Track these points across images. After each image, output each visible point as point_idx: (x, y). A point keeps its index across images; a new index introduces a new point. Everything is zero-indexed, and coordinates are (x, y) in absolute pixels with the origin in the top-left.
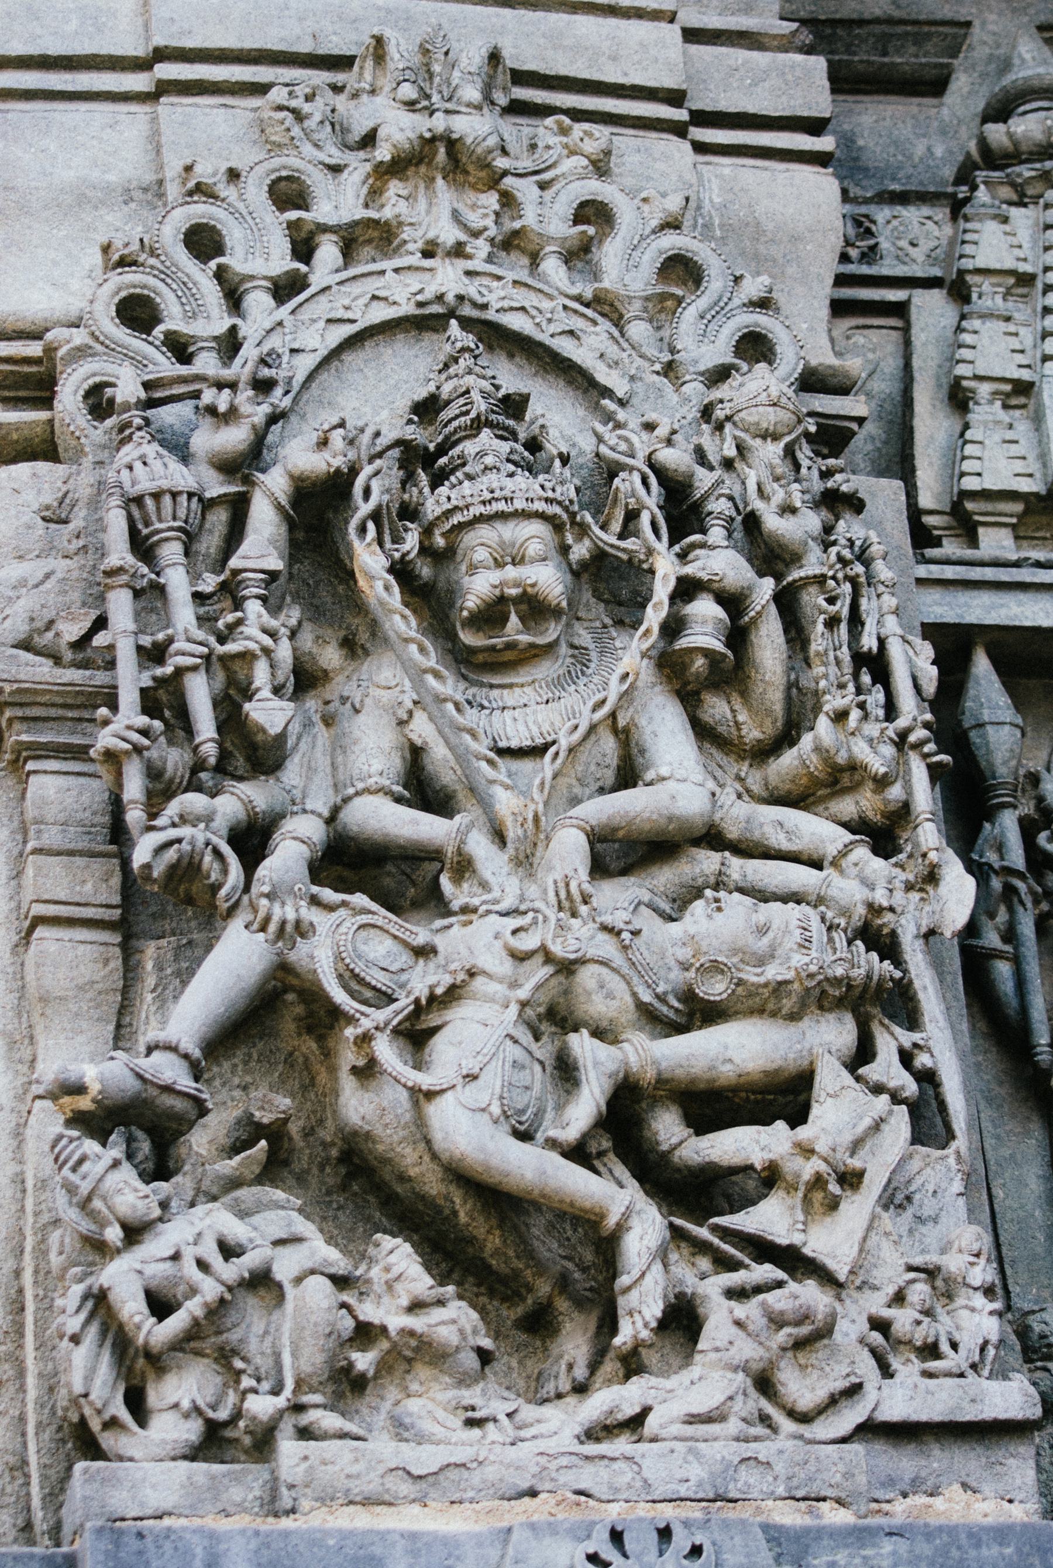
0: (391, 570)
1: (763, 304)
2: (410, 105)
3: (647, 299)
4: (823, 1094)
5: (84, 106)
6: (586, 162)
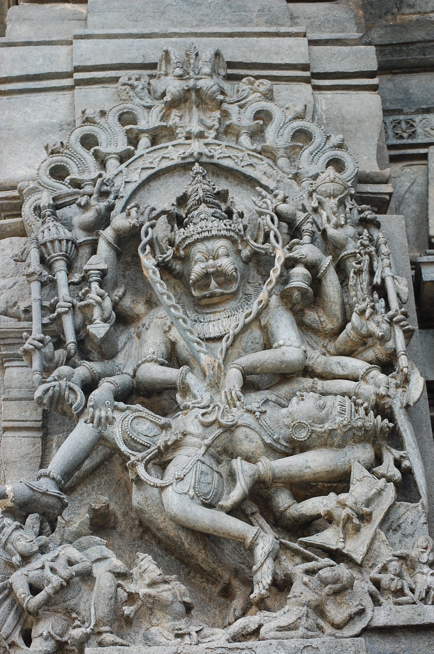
0: (157, 266)
1: (340, 146)
2: (180, 77)
3: (286, 148)
4: (355, 480)
5: (43, 94)
6: (260, 95)
